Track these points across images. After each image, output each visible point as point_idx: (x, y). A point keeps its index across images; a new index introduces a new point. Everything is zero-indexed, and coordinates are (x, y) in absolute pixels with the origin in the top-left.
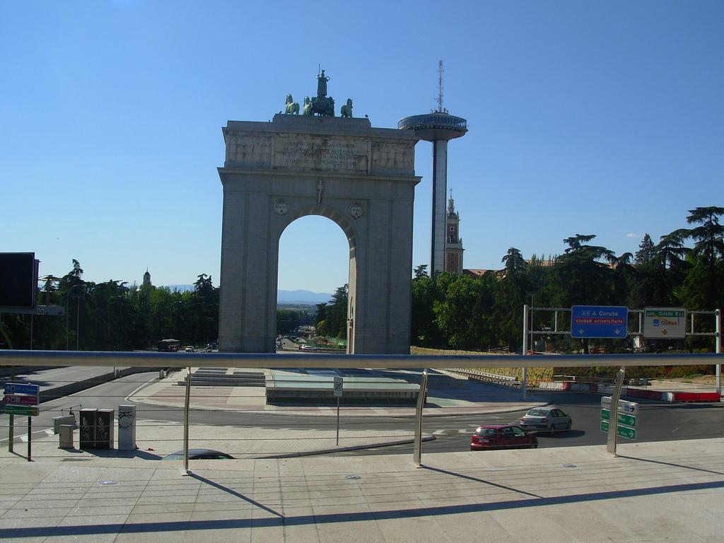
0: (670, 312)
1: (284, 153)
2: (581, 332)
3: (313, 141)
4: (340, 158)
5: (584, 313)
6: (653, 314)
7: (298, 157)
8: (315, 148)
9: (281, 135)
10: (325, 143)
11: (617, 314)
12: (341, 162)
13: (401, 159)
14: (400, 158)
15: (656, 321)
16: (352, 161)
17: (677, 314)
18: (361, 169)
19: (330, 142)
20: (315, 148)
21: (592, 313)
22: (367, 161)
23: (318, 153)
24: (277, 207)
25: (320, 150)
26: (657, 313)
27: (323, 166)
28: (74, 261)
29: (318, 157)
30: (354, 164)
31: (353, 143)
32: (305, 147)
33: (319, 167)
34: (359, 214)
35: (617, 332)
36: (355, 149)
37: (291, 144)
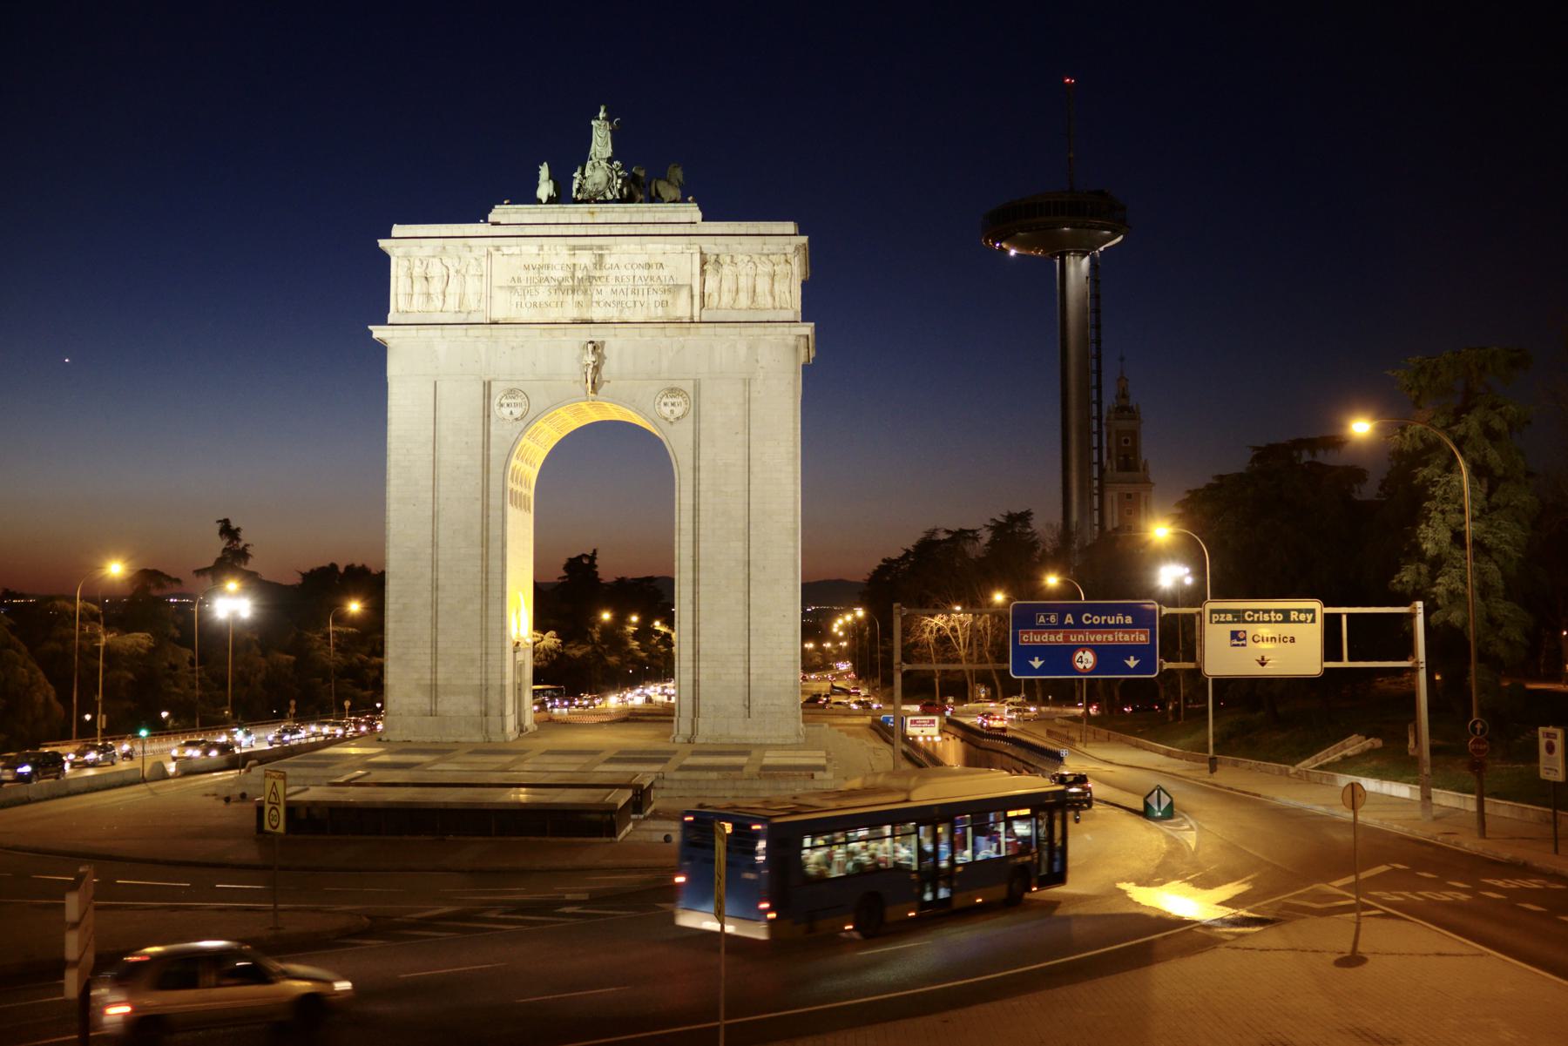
0: (1277, 611)
1: (511, 288)
2: (1037, 664)
3: (573, 261)
4: (633, 292)
5: (1042, 619)
6: (1229, 617)
7: (543, 294)
8: (579, 274)
9: (505, 250)
10: (600, 262)
11: (1129, 620)
12: (635, 302)
13: (767, 288)
14: (763, 285)
15: (1234, 635)
16: (659, 297)
17: (1294, 616)
18: (679, 314)
19: (608, 260)
20: (579, 274)
21: (1062, 618)
22: (692, 297)
23: (581, 284)
24: (502, 405)
25: (590, 279)
26: (1239, 616)
27: (597, 314)
28: (228, 530)
29: (585, 292)
30: (664, 304)
31: (660, 259)
32: (558, 274)
33: (587, 316)
34: (678, 411)
35: (1132, 663)
36: (664, 273)
37: (527, 268)
